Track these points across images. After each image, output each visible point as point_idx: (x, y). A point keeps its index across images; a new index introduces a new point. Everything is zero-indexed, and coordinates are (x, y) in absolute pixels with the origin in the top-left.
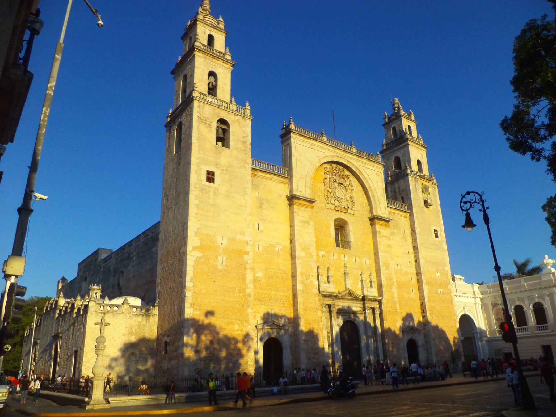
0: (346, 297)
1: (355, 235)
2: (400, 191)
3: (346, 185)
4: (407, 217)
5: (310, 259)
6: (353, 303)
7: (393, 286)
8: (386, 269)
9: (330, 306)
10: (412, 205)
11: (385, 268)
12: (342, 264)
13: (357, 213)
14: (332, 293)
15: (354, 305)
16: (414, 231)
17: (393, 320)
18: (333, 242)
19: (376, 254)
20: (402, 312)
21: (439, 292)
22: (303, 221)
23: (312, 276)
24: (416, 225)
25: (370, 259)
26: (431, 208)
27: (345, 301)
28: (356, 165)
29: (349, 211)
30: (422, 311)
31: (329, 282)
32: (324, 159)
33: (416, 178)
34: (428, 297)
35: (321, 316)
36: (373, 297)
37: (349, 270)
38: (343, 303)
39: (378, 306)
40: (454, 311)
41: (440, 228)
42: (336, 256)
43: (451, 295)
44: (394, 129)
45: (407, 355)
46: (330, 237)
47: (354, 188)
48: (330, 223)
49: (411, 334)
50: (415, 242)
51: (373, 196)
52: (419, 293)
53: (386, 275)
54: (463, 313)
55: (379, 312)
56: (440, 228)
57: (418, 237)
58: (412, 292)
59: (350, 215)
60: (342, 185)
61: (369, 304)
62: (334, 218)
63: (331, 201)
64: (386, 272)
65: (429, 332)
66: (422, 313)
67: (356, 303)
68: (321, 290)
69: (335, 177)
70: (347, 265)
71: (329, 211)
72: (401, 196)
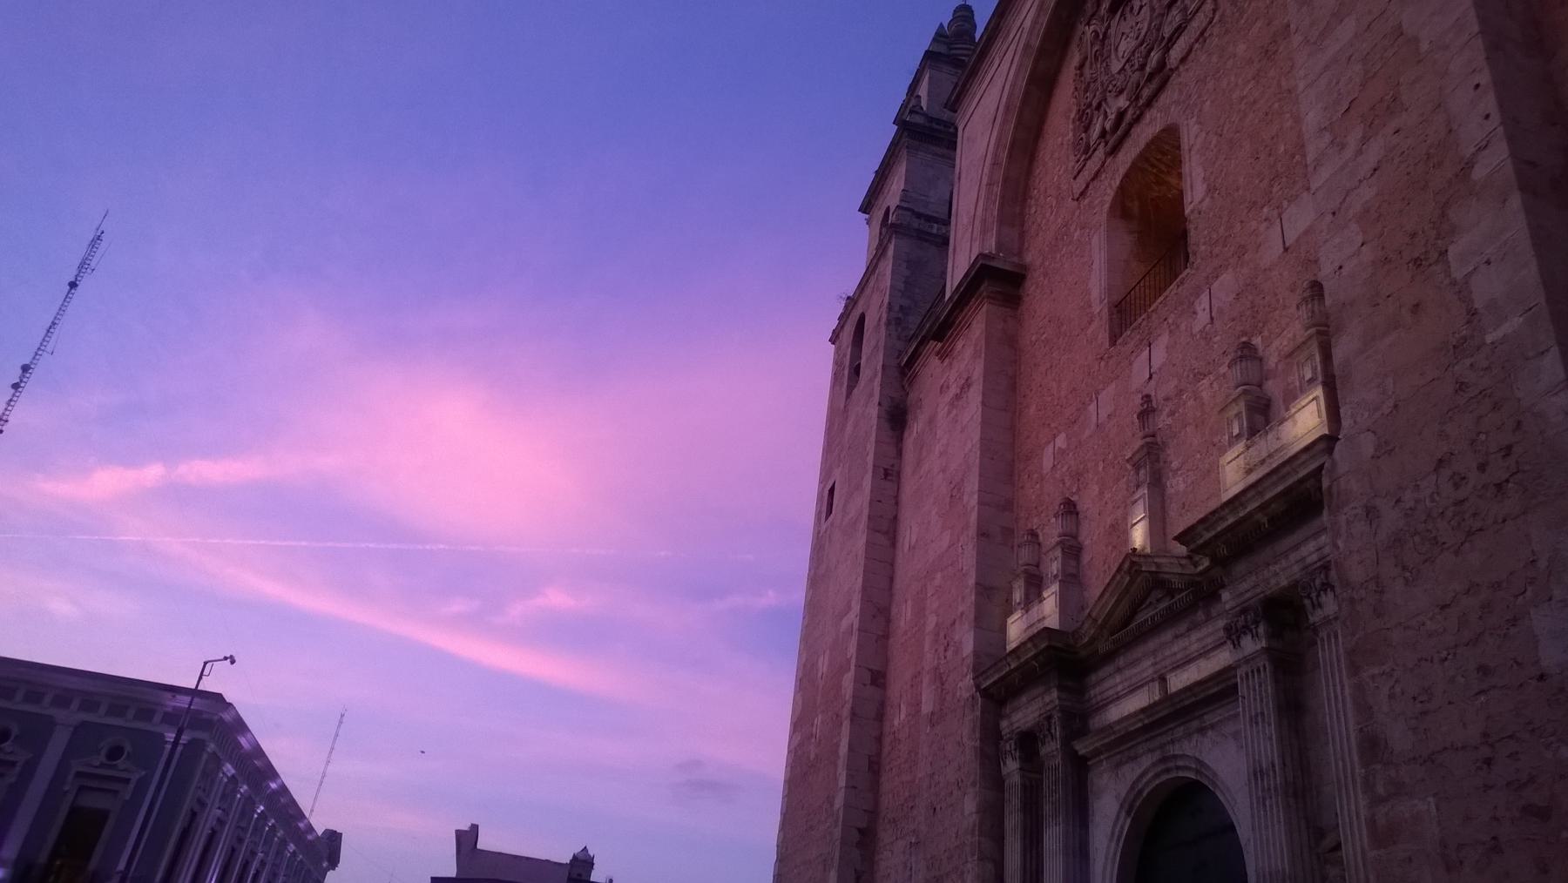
9: (1028, 741)
15: (1193, 642)
23: (962, 614)
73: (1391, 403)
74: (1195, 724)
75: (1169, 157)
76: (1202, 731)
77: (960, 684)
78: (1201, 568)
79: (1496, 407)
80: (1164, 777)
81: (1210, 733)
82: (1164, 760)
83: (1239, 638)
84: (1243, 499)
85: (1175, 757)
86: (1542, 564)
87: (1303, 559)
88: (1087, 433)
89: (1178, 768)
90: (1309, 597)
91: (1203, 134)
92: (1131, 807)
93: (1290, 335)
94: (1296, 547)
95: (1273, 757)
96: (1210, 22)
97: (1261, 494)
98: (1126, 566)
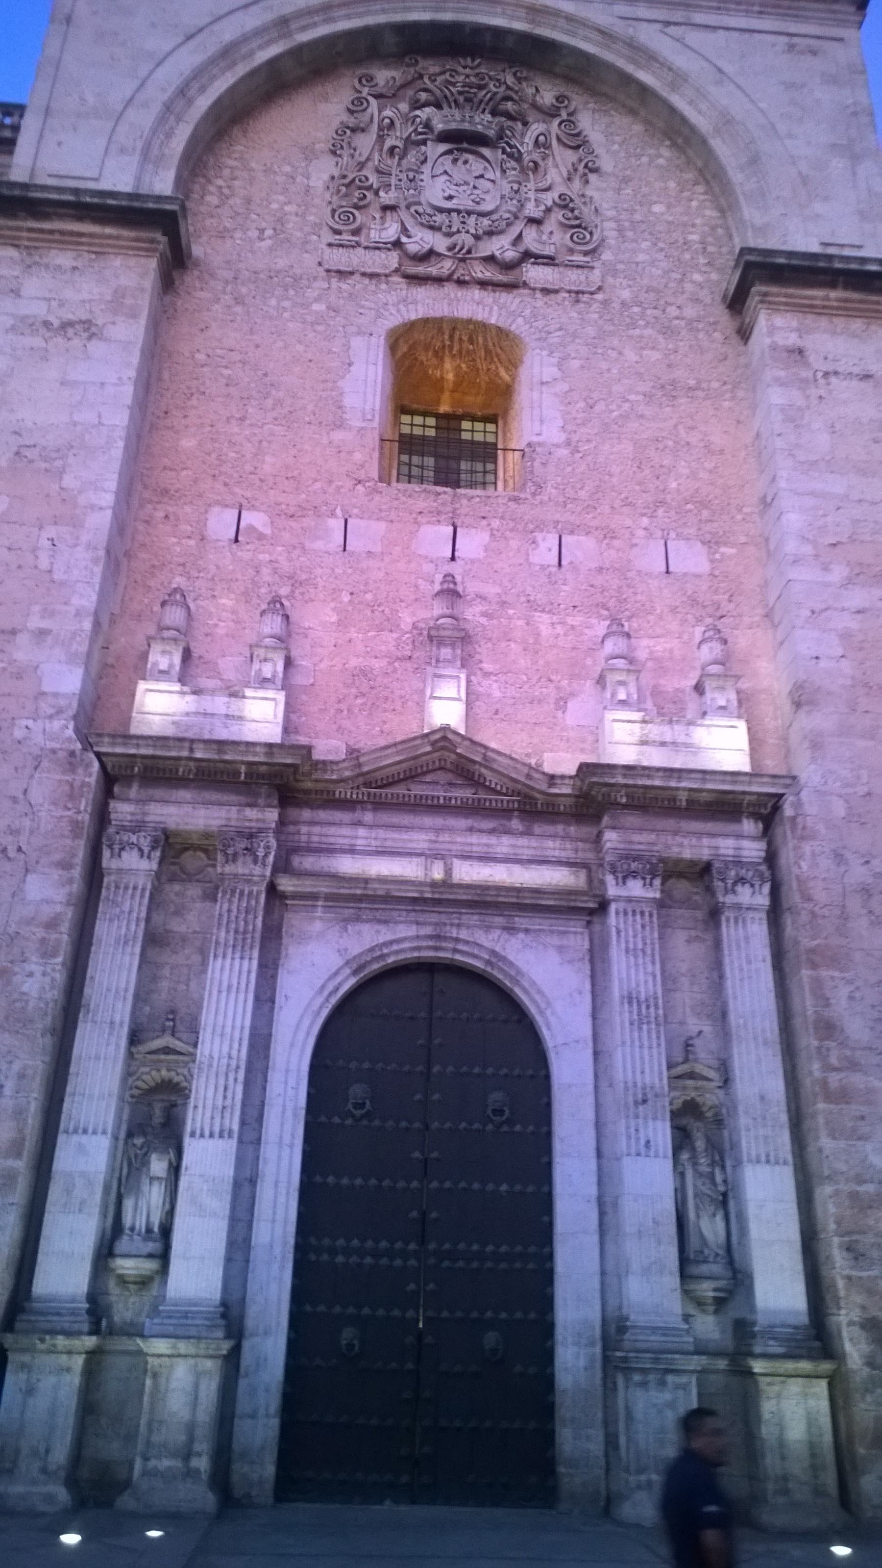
0: (417, 790)
1: (581, 404)
5: (51, 531)
6: (492, 832)
8: (848, 582)
11: (838, 573)
15: (504, 845)
22: (47, 324)
25: (712, 543)
27: (406, 819)
29: (534, 273)
37: (484, 614)
38: (381, 833)
46: (340, 425)
48: (347, 347)
55: (763, 899)
59: (540, 300)
60: (486, 152)
61: (641, 830)
67: (528, 833)
69: (427, 112)
74: (499, 920)
75: (471, 347)
76: (510, 930)
77: (30, 723)
80: (431, 954)
81: (521, 935)
82: (430, 937)
83: (625, 878)
84: (684, 775)
85: (457, 940)
87: (717, 848)
88: (319, 545)
89: (455, 951)
91: (565, 387)
93: (668, 646)
96: (592, 293)
97: (704, 780)
98: (437, 736)
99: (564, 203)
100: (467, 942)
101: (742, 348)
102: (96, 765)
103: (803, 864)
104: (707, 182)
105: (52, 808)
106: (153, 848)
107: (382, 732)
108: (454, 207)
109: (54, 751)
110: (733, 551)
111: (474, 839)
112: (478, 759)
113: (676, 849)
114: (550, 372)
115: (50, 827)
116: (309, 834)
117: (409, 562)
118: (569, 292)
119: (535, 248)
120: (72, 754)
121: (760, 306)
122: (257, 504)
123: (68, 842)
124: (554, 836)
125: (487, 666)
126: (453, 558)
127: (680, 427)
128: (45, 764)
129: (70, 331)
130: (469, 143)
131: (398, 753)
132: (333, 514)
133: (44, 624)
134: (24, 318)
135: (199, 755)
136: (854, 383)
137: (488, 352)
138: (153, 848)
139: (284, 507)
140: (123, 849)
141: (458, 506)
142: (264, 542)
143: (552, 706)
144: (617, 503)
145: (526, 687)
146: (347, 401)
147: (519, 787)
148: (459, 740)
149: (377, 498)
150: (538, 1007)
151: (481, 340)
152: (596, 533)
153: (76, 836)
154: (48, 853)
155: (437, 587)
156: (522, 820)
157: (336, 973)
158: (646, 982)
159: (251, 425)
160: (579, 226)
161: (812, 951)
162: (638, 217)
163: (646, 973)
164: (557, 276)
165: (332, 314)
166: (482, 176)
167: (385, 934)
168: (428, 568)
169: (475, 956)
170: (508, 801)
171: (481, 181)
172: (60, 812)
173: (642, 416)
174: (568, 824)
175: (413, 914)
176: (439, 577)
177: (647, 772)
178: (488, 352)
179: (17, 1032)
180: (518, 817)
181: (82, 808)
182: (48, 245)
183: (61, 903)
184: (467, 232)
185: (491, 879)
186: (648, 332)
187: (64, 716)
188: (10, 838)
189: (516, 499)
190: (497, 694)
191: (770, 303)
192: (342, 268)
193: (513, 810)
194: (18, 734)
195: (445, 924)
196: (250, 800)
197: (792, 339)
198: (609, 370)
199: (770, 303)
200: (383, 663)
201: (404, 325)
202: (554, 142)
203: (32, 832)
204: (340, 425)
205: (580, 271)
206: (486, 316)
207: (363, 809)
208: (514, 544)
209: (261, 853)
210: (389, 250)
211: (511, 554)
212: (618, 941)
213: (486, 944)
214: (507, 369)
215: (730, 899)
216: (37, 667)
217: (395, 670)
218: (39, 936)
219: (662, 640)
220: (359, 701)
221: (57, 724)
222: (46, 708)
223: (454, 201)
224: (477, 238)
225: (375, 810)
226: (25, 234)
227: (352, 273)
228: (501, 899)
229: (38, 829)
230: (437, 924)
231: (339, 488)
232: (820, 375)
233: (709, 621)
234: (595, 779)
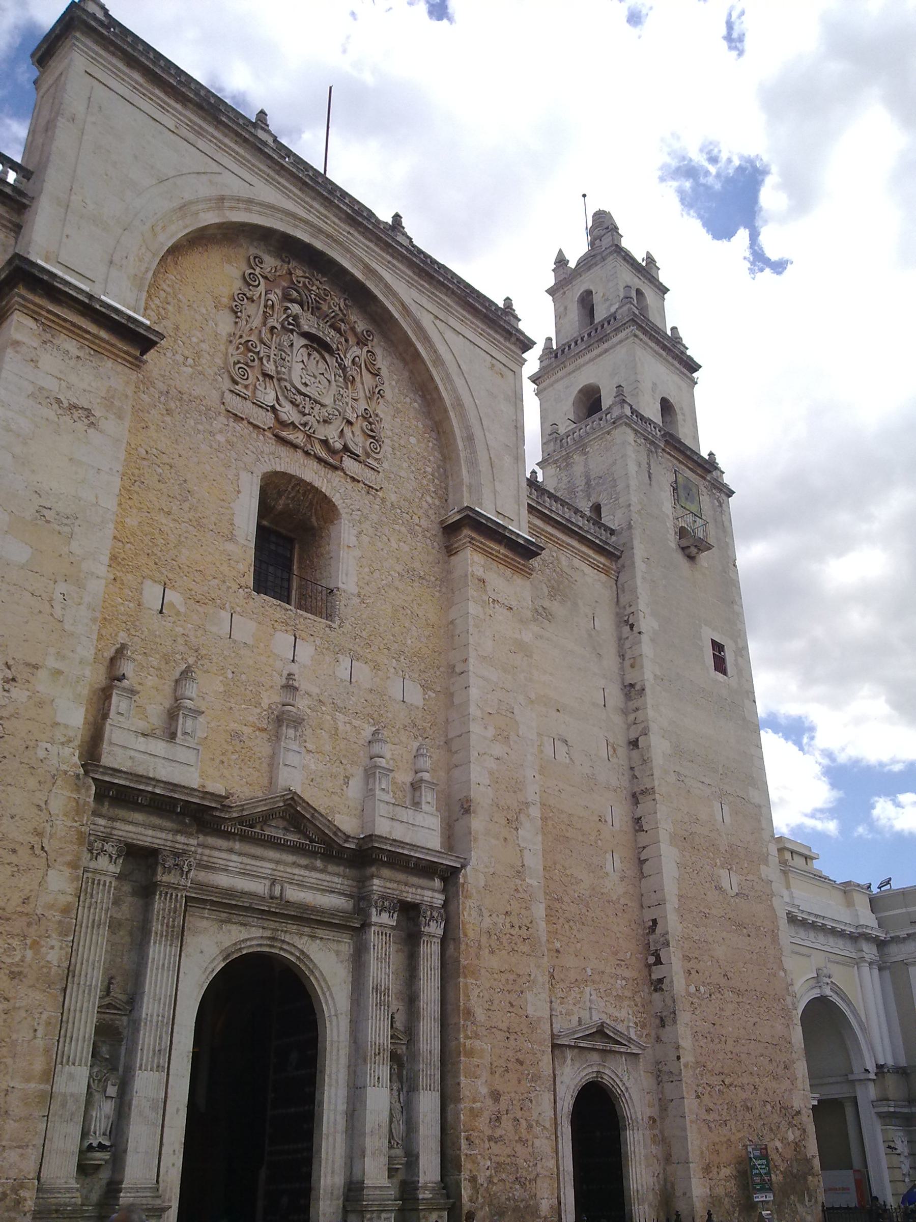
1: (367, 570)
2: (588, 484)
3: (348, 362)
4: (606, 572)
6: (306, 867)
7: (522, 817)
8: (494, 739)
10: (630, 527)
11: (491, 732)
12: (276, 677)
13: (385, 485)
14: (175, 786)
16: (632, 626)
17: (512, 977)
18: (242, 567)
19: (458, 670)
20: (558, 951)
21: (725, 884)
23: (59, 672)
24: (643, 604)
26: (704, 558)
28: (407, 300)
29: (348, 463)
30: (652, 960)
31: (172, 736)
32: (250, 211)
33: (652, 443)
34: (680, 897)
35: (64, 900)
36: (414, 847)
39: (438, 899)
40: (782, 974)
41: (736, 642)
42: (246, 629)
43: (771, 906)
44: (587, 302)
45: (568, 1164)
46: (232, 538)
47: (386, 387)
48: (238, 475)
49: (595, 1057)
50: (632, 666)
51: (470, 438)
52: (642, 875)
53: (491, 764)
54: (815, 993)
56: (736, 642)
57: (647, 648)
58: (609, 868)
61: (391, 880)
62: (267, 468)
63: (258, 393)
64: (498, 749)
65: (679, 1058)
66: (649, 966)
68: (106, 760)
70: (302, 683)
71: (241, 428)
72: (593, 500)
73: (492, 870)
74: (307, 929)
76: (313, 937)
77: (48, 746)
78: (346, 845)
79: (526, 908)
80: (267, 949)
81: (318, 941)
82: (269, 938)
83: (381, 911)
85: (283, 941)
86: (532, 977)
87: (423, 896)
89: (281, 949)
90: (425, 917)
92: (228, 955)
94: (423, 888)
95: (389, 984)
96: (377, 490)
99: (366, 416)
100: (289, 943)
101: (447, 558)
102: (94, 788)
103: (465, 913)
104: (439, 433)
105: (65, 819)
106: (119, 856)
107: (247, 783)
108: (308, 394)
109: (66, 772)
110: (434, 695)
111: (296, 871)
112: (308, 816)
113: (405, 895)
114: (353, 540)
115: (63, 834)
116: (202, 854)
117: (269, 657)
118: (366, 485)
119: (351, 446)
120: (78, 775)
121: (468, 544)
122: (176, 585)
123: (76, 847)
124: (338, 875)
125: (310, 746)
126: (293, 661)
127: (414, 602)
128: (59, 782)
129: (76, 414)
130: (318, 345)
131: (265, 805)
132: (223, 608)
133: (58, 665)
134: (41, 389)
135: (158, 791)
136: (505, 611)
137: (311, 504)
138: (119, 856)
139: (194, 593)
140: (98, 854)
141: (298, 622)
142: (180, 618)
143: (342, 782)
144: (382, 646)
145: (329, 764)
146: (237, 521)
147: (327, 838)
148: (301, 802)
149: (251, 602)
150: (322, 990)
151: (310, 496)
152: (371, 664)
153: (81, 844)
154: (62, 855)
155: (284, 681)
156: (322, 860)
157: (214, 959)
158: (385, 978)
159: (174, 520)
160: (373, 437)
161: (465, 967)
162: (402, 443)
163: (385, 974)
164: (360, 471)
165: (229, 447)
166: (323, 374)
167: (244, 935)
168: (279, 664)
169: (292, 954)
170: (318, 847)
171: (322, 376)
172: (69, 823)
173: (397, 589)
174: (346, 867)
175: (260, 921)
176: (285, 673)
177: (402, 845)
178: (311, 504)
179: (45, 991)
180: (320, 858)
181: (85, 822)
182: (60, 329)
183: (71, 894)
184: (314, 416)
185: (304, 900)
186: (403, 529)
187: (71, 745)
188: (37, 838)
189: (330, 627)
190: (313, 767)
191: (473, 544)
192: (239, 414)
193: (318, 853)
194: (41, 754)
195: (278, 930)
196: (180, 828)
197: (480, 572)
198: (382, 549)
199: (473, 544)
200: (250, 730)
201: (272, 472)
202: (363, 365)
203: (51, 836)
204: (232, 538)
205: (372, 472)
206: (320, 485)
207: (235, 840)
208: (327, 658)
209: (186, 869)
210: (268, 411)
211: (325, 666)
212: (374, 953)
213: (299, 946)
214: (318, 519)
215: (426, 930)
216: (53, 700)
217: (256, 737)
218: (58, 918)
219: (397, 747)
220: (234, 757)
221: (67, 751)
222: (59, 736)
223: (308, 388)
224: (318, 422)
225: (241, 841)
226: (44, 313)
227: (242, 419)
228: (312, 917)
229: (55, 833)
230: (273, 929)
231: (229, 588)
232: (491, 600)
233: (420, 738)
234: (376, 845)
